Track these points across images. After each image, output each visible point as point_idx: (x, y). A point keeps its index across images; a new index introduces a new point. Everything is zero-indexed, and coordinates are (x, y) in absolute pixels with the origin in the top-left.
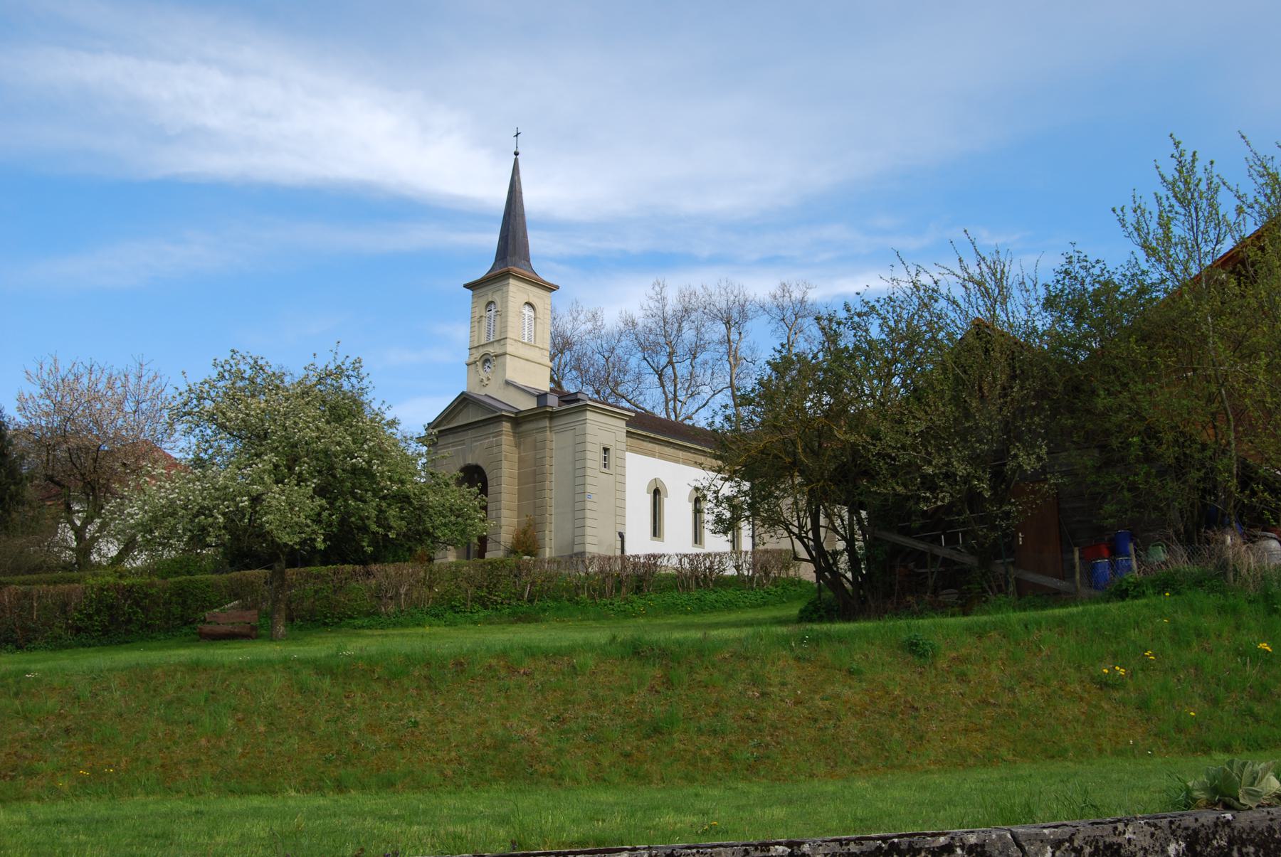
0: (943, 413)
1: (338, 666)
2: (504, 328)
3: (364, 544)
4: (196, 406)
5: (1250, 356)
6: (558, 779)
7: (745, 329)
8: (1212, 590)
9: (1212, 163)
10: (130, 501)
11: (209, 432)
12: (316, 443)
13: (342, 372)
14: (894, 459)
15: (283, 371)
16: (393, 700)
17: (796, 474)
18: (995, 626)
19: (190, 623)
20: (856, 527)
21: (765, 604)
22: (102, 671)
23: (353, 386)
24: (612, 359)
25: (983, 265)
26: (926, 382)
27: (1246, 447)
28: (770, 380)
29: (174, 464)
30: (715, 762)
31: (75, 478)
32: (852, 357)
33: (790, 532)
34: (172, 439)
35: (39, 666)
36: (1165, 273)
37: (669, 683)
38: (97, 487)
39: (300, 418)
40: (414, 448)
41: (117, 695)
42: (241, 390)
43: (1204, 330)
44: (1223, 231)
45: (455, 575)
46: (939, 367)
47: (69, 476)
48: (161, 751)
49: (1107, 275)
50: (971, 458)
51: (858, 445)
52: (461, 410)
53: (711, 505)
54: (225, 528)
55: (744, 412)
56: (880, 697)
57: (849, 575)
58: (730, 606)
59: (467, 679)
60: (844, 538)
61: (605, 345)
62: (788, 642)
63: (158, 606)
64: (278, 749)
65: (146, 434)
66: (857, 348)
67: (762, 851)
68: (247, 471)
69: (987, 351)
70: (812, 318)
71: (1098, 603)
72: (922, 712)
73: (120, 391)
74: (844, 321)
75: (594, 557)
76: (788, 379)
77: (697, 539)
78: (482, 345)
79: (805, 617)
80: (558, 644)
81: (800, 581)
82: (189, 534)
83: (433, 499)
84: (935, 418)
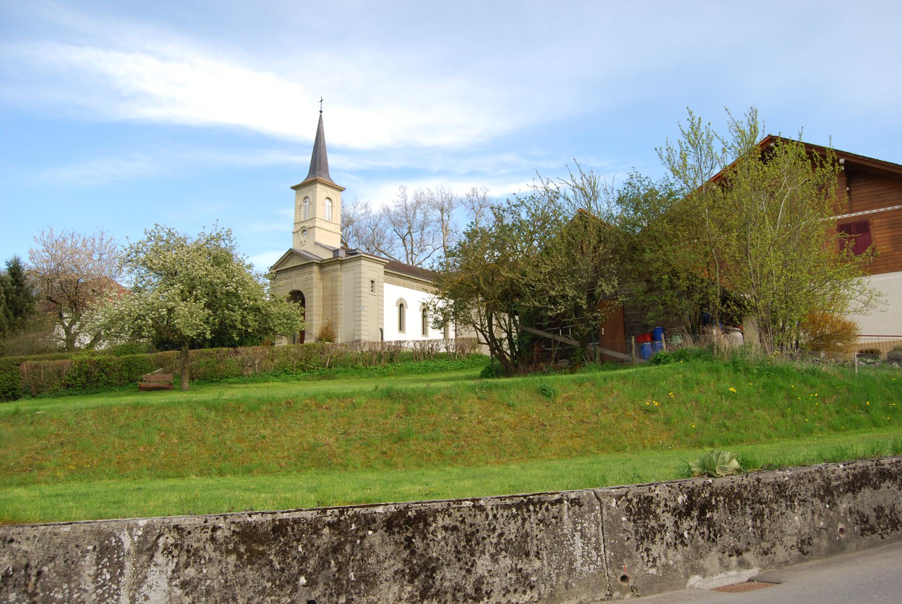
0: (561, 261)
1: (219, 405)
2: (314, 212)
3: (234, 335)
4: (135, 256)
5: (728, 231)
6: (345, 467)
8: (706, 359)
9: (709, 124)
10: (97, 311)
11: (143, 271)
13: (220, 237)
14: (534, 287)
15: (186, 236)
16: (251, 424)
17: (480, 295)
18: (588, 380)
19: (134, 381)
20: (513, 325)
21: (462, 368)
22: (82, 409)
24: (376, 230)
25: (584, 179)
26: (552, 244)
27: (725, 281)
28: (465, 243)
29: (123, 290)
30: (433, 456)
32: (511, 230)
33: (476, 328)
34: (121, 276)
35: (44, 407)
36: (683, 185)
37: (408, 413)
38: (77, 303)
40: (262, 281)
41: (91, 423)
43: (704, 216)
44: (714, 162)
45: (287, 353)
47: (61, 297)
48: (117, 454)
49: (652, 185)
51: (514, 279)
52: (289, 259)
55: (451, 260)
56: (525, 419)
57: (509, 352)
58: (442, 369)
59: (293, 412)
60: (506, 331)
61: (372, 222)
62: (474, 389)
63: (115, 372)
64: (184, 453)
65: (106, 273)
66: (514, 225)
67: (458, 504)
68: (165, 294)
69: (586, 227)
70: (489, 208)
71: (644, 366)
72: (548, 427)
73: (90, 248)
74: (506, 209)
75: (366, 343)
76: (475, 242)
77: (424, 332)
79: (484, 375)
80: (345, 391)
81: (481, 355)
83: (274, 310)
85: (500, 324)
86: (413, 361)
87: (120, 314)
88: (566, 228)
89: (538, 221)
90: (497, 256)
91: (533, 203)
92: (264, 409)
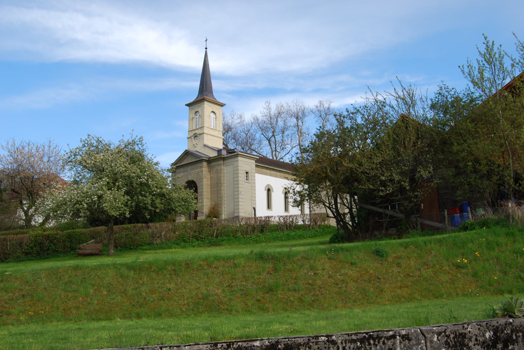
0: (389, 154)
1: (136, 266)
2: (203, 123)
3: (146, 215)
4: (74, 158)
5: (518, 127)
6: (230, 311)
7: (305, 120)
8: (503, 226)
9: (501, 46)
10: (47, 199)
11: (80, 169)
12: (125, 173)
13: (135, 142)
14: (368, 174)
15: (110, 143)
16: (160, 280)
17: (327, 181)
18: (412, 243)
19: (74, 249)
20: (353, 203)
21: (315, 236)
22: (37, 271)
23: (140, 148)
24: (249, 134)
25: (404, 91)
26: (381, 141)
27: (516, 166)
28: (315, 142)
29: (65, 183)
30: (296, 302)
31: (24, 190)
32: (350, 131)
33: (325, 205)
34: (64, 172)
35: (11, 269)
36: (481, 93)
37: (275, 270)
39: (118, 162)
40: (166, 174)
41: (44, 280)
42: (92, 151)
43: (498, 117)
44: (506, 75)
45: (185, 227)
46: (387, 135)
47: (21, 189)
48: (63, 303)
49: (457, 94)
50: (401, 173)
51: (353, 168)
52: (185, 158)
53: (292, 195)
54: (87, 209)
55: (305, 155)
56: (364, 274)
57: (350, 223)
58: (301, 237)
59: (191, 270)
60: (348, 208)
61: (245, 129)
62: (325, 252)
63: (60, 243)
64: (112, 302)
65: (53, 171)
66: (352, 128)
67: (315, 339)
68: (96, 185)
69: (407, 128)
70: (332, 115)
71: (455, 232)
72: (382, 280)
73: (41, 153)
74: (346, 116)
75: (243, 218)
76: (323, 141)
77: (286, 209)
78: (194, 130)
79: (333, 241)
81: (330, 226)
82: (72, 212)
83: (175, 195)
84: (385, 156)
85: (343, 202)
86: (279, 231)
87: (64, 201)
88: (392, 129)
89: (370, 124)
90: (340, 151)
91: (366, 111)
92: (169, 268)
